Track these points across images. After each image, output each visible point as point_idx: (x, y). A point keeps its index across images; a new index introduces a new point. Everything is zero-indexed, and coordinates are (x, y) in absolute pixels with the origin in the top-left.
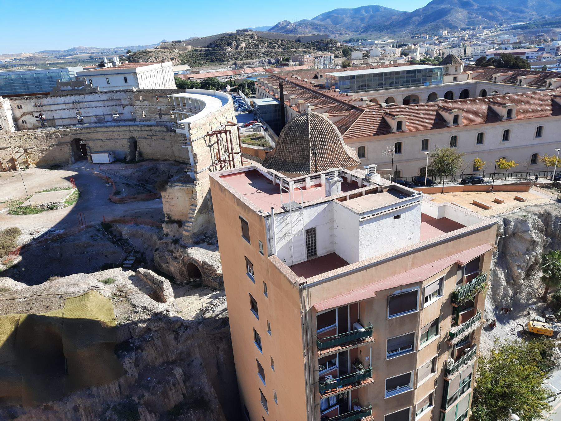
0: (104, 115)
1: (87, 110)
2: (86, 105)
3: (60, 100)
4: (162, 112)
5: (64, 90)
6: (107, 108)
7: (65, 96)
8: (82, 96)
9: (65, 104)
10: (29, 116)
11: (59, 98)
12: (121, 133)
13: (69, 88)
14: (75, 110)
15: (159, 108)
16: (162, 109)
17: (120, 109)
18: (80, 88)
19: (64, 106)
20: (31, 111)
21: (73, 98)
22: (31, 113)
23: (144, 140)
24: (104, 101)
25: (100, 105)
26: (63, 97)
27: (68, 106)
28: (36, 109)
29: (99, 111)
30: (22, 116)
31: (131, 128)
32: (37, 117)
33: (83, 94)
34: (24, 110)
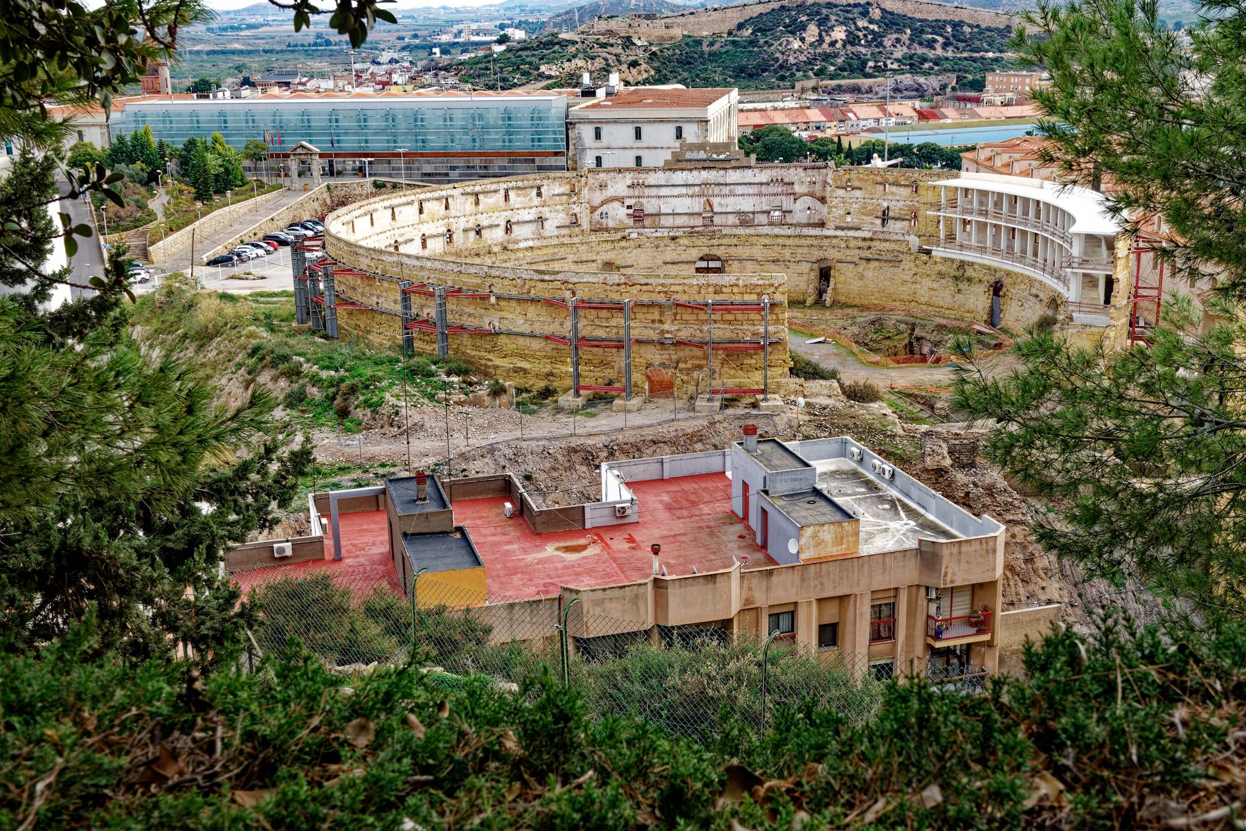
0: (753, 213)
1: (724, 201)
2: (726, 190)
3: (679, 177)
4: (891, 214)
5: (690, 160)
6: (764, 199)
7: (691, 170)
8: (722, 172)
9: (687, 185)
10: (617, 204)
11: (679, 173)
12: (800, 251)
13: (702, 155)
14: (703, 200)
15: (885, 204)
16: (892, 207)
17: (787, 203)
18: (722, 157)
19: (684, 190)
20: (623, 194)
21: (705, 175)
22: (621, 200)
23: (851, 266)
24: (762, 184)
25: (751, 191)
26: (685, 173)
27: (691, 191)
28: (631, 192)
29: (746, 205)
30: (603, 203)
31: (826, 242)
32: (629, 207)
33: (725, 169)
34: (610, 192)
